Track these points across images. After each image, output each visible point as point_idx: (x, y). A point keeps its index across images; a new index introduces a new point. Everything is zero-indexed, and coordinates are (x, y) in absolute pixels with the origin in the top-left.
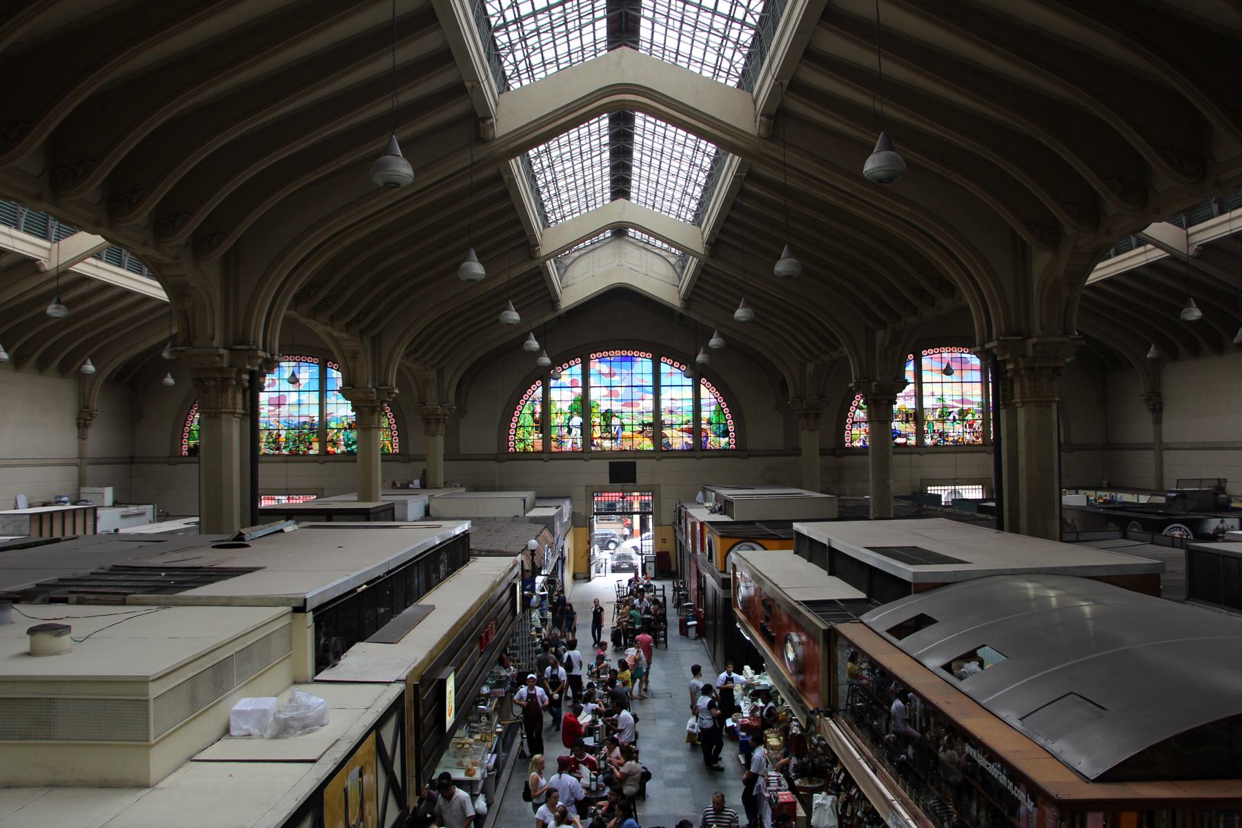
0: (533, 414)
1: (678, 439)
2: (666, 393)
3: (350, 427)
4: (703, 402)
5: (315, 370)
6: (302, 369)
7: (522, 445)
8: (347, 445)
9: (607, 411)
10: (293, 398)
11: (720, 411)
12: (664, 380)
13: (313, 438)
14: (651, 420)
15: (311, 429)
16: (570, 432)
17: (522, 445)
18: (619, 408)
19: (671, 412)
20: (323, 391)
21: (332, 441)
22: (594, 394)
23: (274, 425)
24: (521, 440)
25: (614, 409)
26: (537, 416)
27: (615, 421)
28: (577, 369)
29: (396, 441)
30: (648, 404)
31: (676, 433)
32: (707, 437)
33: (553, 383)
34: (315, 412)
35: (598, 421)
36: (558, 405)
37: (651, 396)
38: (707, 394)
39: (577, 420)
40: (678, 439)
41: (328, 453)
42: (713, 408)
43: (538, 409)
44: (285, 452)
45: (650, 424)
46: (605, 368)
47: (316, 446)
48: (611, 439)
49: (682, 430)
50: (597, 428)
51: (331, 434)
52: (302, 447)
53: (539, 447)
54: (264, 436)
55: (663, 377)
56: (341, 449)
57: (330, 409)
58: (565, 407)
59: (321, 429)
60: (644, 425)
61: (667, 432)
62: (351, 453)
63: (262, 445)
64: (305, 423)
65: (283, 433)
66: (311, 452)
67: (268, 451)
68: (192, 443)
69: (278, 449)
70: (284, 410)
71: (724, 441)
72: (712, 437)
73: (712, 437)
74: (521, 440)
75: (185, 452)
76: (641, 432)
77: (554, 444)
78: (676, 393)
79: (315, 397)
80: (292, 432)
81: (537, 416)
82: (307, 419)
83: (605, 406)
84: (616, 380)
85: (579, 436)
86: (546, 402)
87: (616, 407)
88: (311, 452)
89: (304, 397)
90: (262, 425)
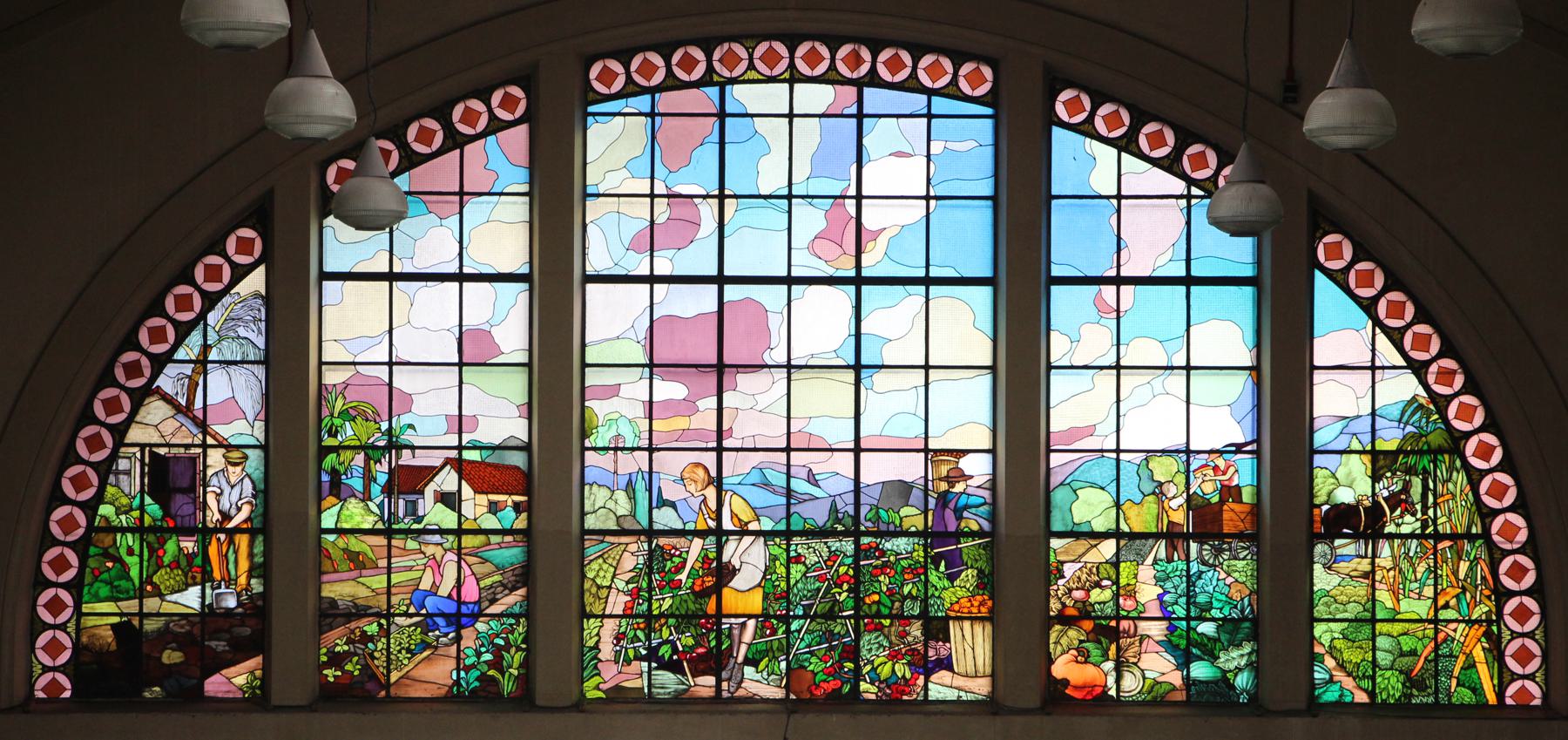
3: (1206, 523)
5: (969, 143)
6: (879, 135)
8: (1185, 650)
10: (821, 321)
13: (955, 592)
15: (931, 536)
20: (1022, 282)
21: (1085, 611)
23: (684, 502)
29: (1524, 624)
34: (966, 415)
41: (1056, 694)
44: (759, 684)
47: (972, 646)
51: (1073, 564)
52: (873, 649)
54: (613, 574)
56: (1158, 666)
57: (1073, 404)
59: (1005, 532)
62: (1217, 694)
63: (603, 634)
64: (902, 489)
65: (749, 559)
66: (941, 688)
67: (636, 677)
68: (103, 614)
69: (715, 662)
70: (755, 406)
75: (50, 673)
79: (966, 326)
80: (813, 552)
82: (911, 468)
88: (941, 688)
89: (893, 320)
90: (603, 506)
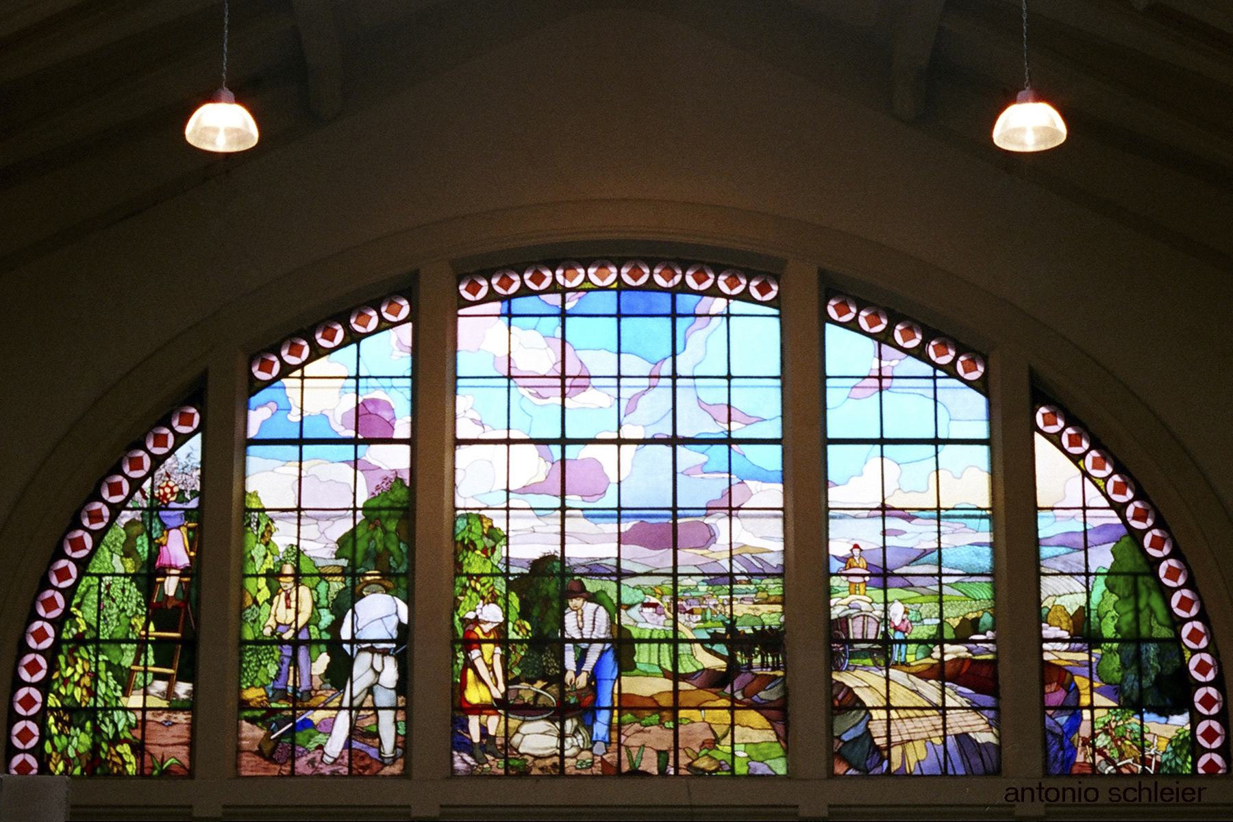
0: (149, 575)
1: (914, 719)
2: (852, 479)
4: (1047, 527)
7: (81, 741)
9: (541, 566)
11: (1134, 575)
12: (846, 413)
14: (772, 616)
16: (340, 673)
17: (81, 741)
18: (606, 550)
19: (882, 576)
22: (477, 480)
24: (74, 714)
25: (576, 552)
26: (171, 585)
27: (584, 621)
28: (388, 351)
30: (764, 537)
31: (903, 687)
32: (1075, 711)
33: (258, 419)
35: (492, 614)
36: (284, 536)
37: (772, 494)
38: (1064, 482)
39: (380, 613)
40: (914, 719)
42: (1102, 558)
43: (177, 549)
45: (768, 640)
46: (533, 346)
48: (558, 713)
49: (940, 673)
50: (488, 656)
53: (177, 756)
55: (835, 395)
58: (321, 544)
60: (732, 638)
61: (864, 681)
71: (1164, 730)
72: (1099, 708)
73: (1099, 708)
74: (74, 714)
76: (715, 681)
77: (251, 733)
78: (910, 479)
81: (171, 585)
83: (529, 542)
84: (591, 412)
85: (385, 697)
86: (222, 513)
87: (591, 544)
